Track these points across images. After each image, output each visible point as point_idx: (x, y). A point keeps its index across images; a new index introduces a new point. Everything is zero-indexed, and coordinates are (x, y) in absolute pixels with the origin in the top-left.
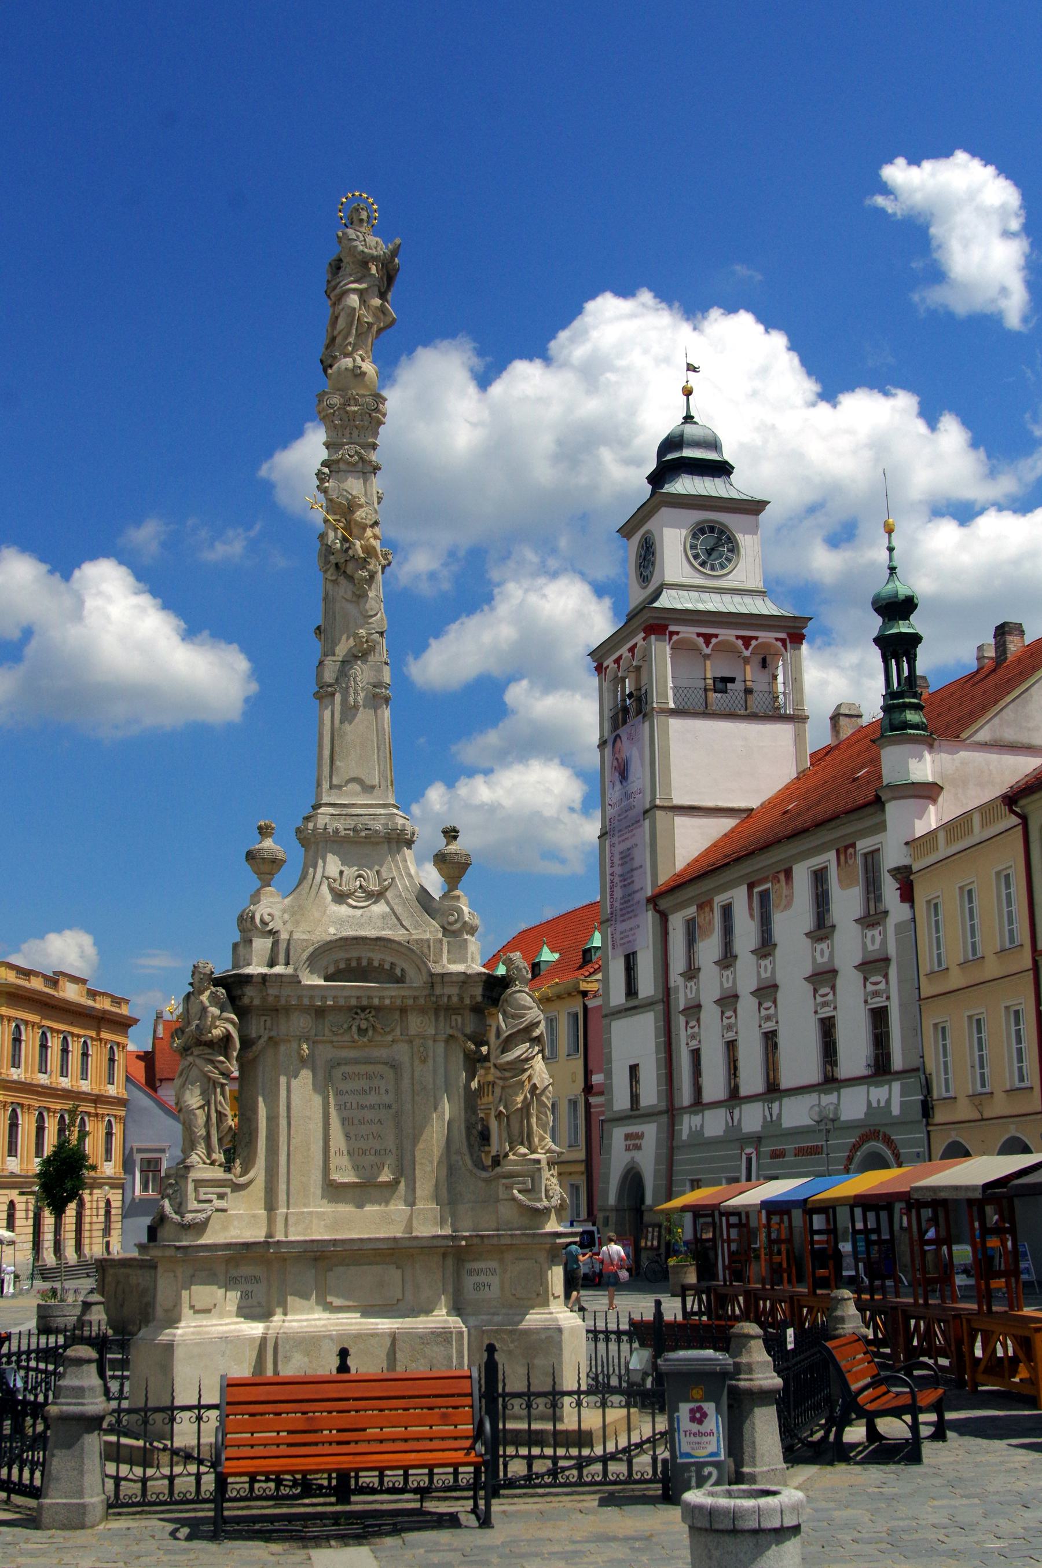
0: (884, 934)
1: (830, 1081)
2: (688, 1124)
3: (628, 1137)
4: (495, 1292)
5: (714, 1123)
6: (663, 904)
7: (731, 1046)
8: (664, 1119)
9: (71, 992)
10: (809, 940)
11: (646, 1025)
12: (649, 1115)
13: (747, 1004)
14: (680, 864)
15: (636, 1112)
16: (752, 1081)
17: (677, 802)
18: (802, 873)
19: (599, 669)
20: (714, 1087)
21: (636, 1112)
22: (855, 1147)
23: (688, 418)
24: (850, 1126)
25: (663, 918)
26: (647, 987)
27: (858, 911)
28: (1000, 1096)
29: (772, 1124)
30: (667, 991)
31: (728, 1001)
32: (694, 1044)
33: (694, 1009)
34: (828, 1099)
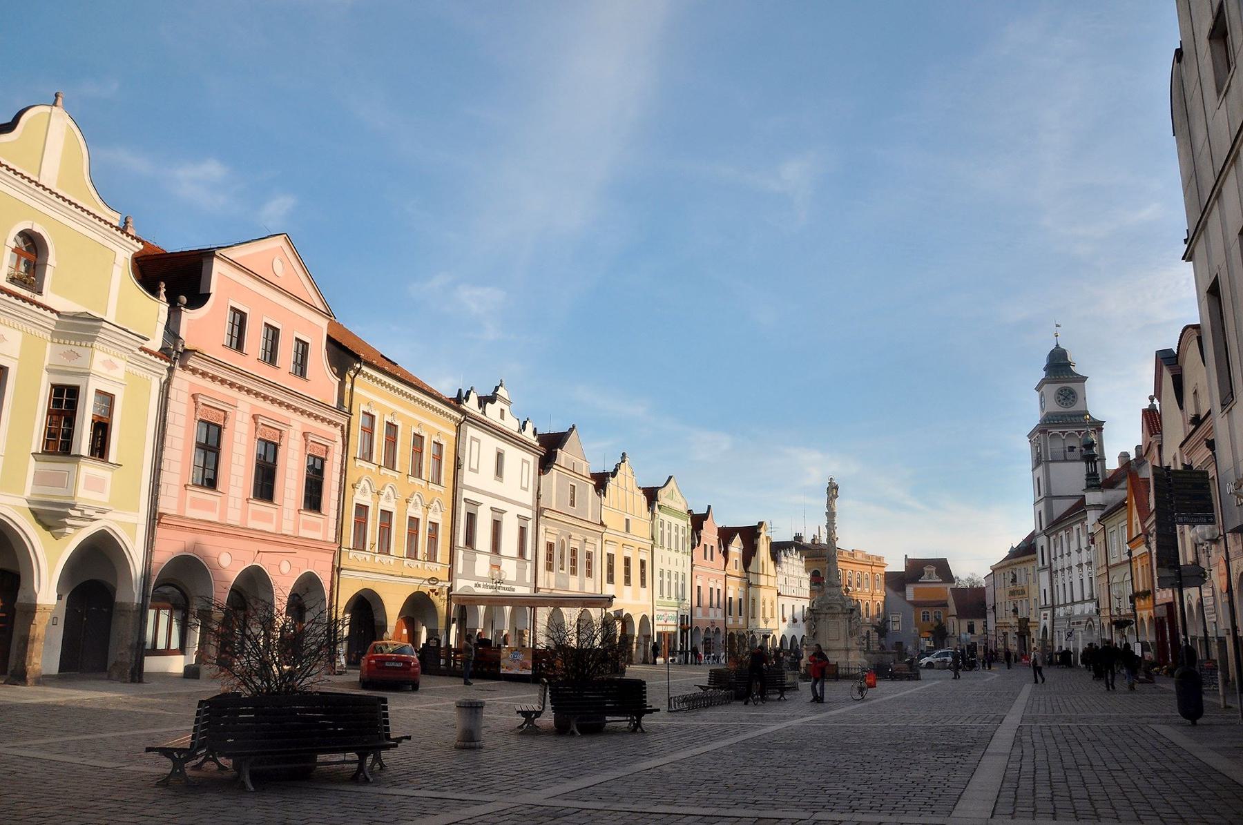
1: (1083, 601)
2: (1057, 610)
3: (1045, 615)
4: (853, 656)
5: (1061, 612)
8: (1051, 609)
9: (859, 557)
11: (1044, 577)
13: (1066, 571)
15: (1045, 607)
17: (1054, 495)
18: (1075, 527)
19: (1030, 441)
21: (1045, 607)
23: (1057, 345)
25: (1048, 537)
26: (1046, 563)
30: (1051, 564)
31: (1063, 570)
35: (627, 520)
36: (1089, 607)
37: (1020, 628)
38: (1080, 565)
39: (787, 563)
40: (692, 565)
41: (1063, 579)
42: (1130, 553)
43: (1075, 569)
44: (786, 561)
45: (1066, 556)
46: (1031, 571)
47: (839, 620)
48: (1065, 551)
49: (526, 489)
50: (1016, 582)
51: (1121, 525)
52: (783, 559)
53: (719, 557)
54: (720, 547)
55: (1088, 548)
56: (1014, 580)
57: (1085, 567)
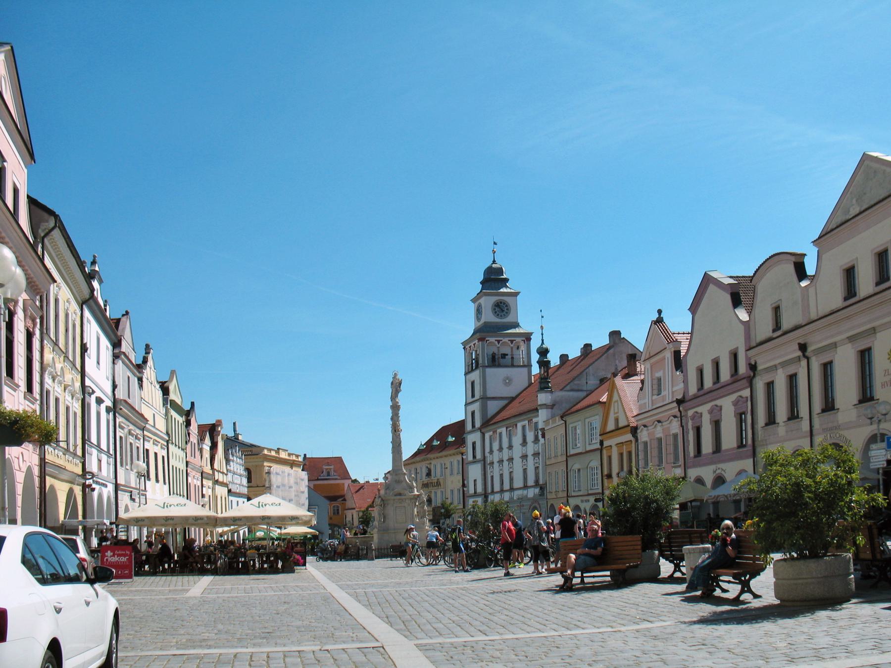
0: (539, 446)
1: (526, 487)
2: (491, 498)
6: (483, 431)
7: (501, 475)
9: (283, 455)
10: (521, 447)
12: (479, 495)
13: (506, 463)
14: (489, 416)
15: (476, 494)
16: (507, 486)
17: (488, 396)
18: (520, 425)
20: (497, 488)
21: (476, 494)
22: (530, 506)
24: (529, 499)
25: (483, 435)
26: (479, 456)
27: (533, 440)
28: (560, 492)
29: (511, 498)
31: (501, 461)
32: (492, 474)
33: (492, 463)
34: (525, 492)
35: (154, 415)
36: (532, 493)
37: (433, 516)
38: (524, 457)
39: (233, 461)
40: (187, 462)
41: (501, 470)
42: (602, 443)
43: (518, 462)
44: (232, 458)
45: (505, 450)
46: (448, 465)
47: (406, 505)
48: (505, 444)
49: (108, 379)
50: (431, 475)
51: (587, 421)
52: (231, 457)
53: (198, 453)
54: (198, 444)
55: (536, 440)
56: (429, 474)
57: (530, 459)
